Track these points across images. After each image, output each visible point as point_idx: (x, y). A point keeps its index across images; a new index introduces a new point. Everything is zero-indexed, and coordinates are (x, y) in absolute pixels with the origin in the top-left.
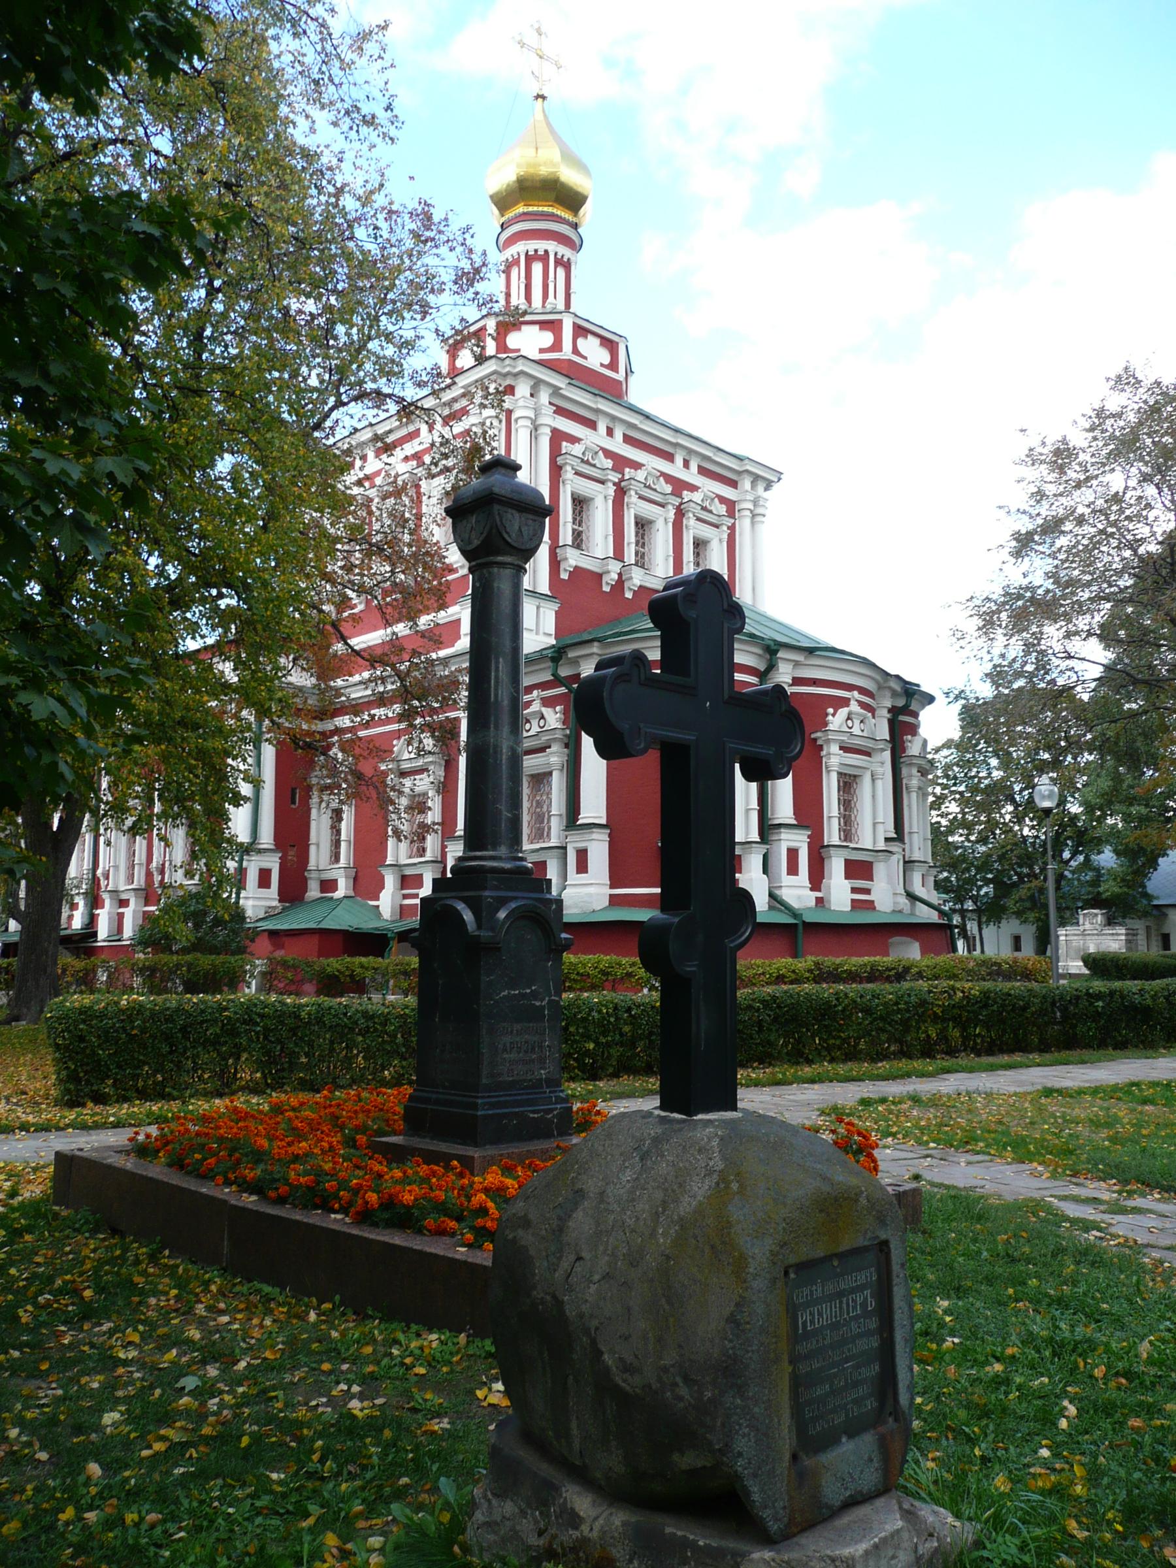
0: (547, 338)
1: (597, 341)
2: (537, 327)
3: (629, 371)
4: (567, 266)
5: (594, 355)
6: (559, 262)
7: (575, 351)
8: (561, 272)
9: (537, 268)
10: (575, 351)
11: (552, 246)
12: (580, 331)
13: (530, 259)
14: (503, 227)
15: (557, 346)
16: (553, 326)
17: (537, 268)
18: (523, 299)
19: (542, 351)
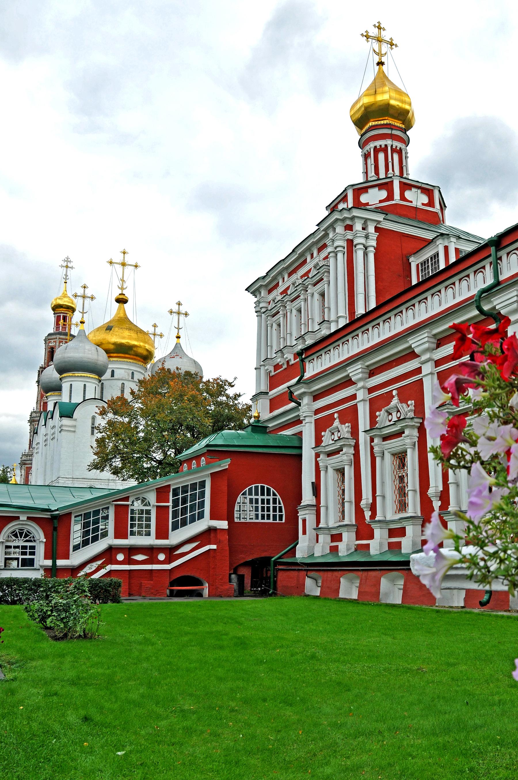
0: (384, 194)
1: (419, 191)
2: (376, 189)
3: (443, 206)
4: (400, 152)
5: (417, 199)
6: (393, 150)
7: (403, 198)
8: (396, 157)
9: (381, 156)
10: (403, 198)
11: (389, 142)
12: (405, 186)
13: (377, 151)
14: (362, 136)
15: (390, 197)
16: (387, 186)
17: (381, 156)
18: (373, 174)
19: (381, 201)
